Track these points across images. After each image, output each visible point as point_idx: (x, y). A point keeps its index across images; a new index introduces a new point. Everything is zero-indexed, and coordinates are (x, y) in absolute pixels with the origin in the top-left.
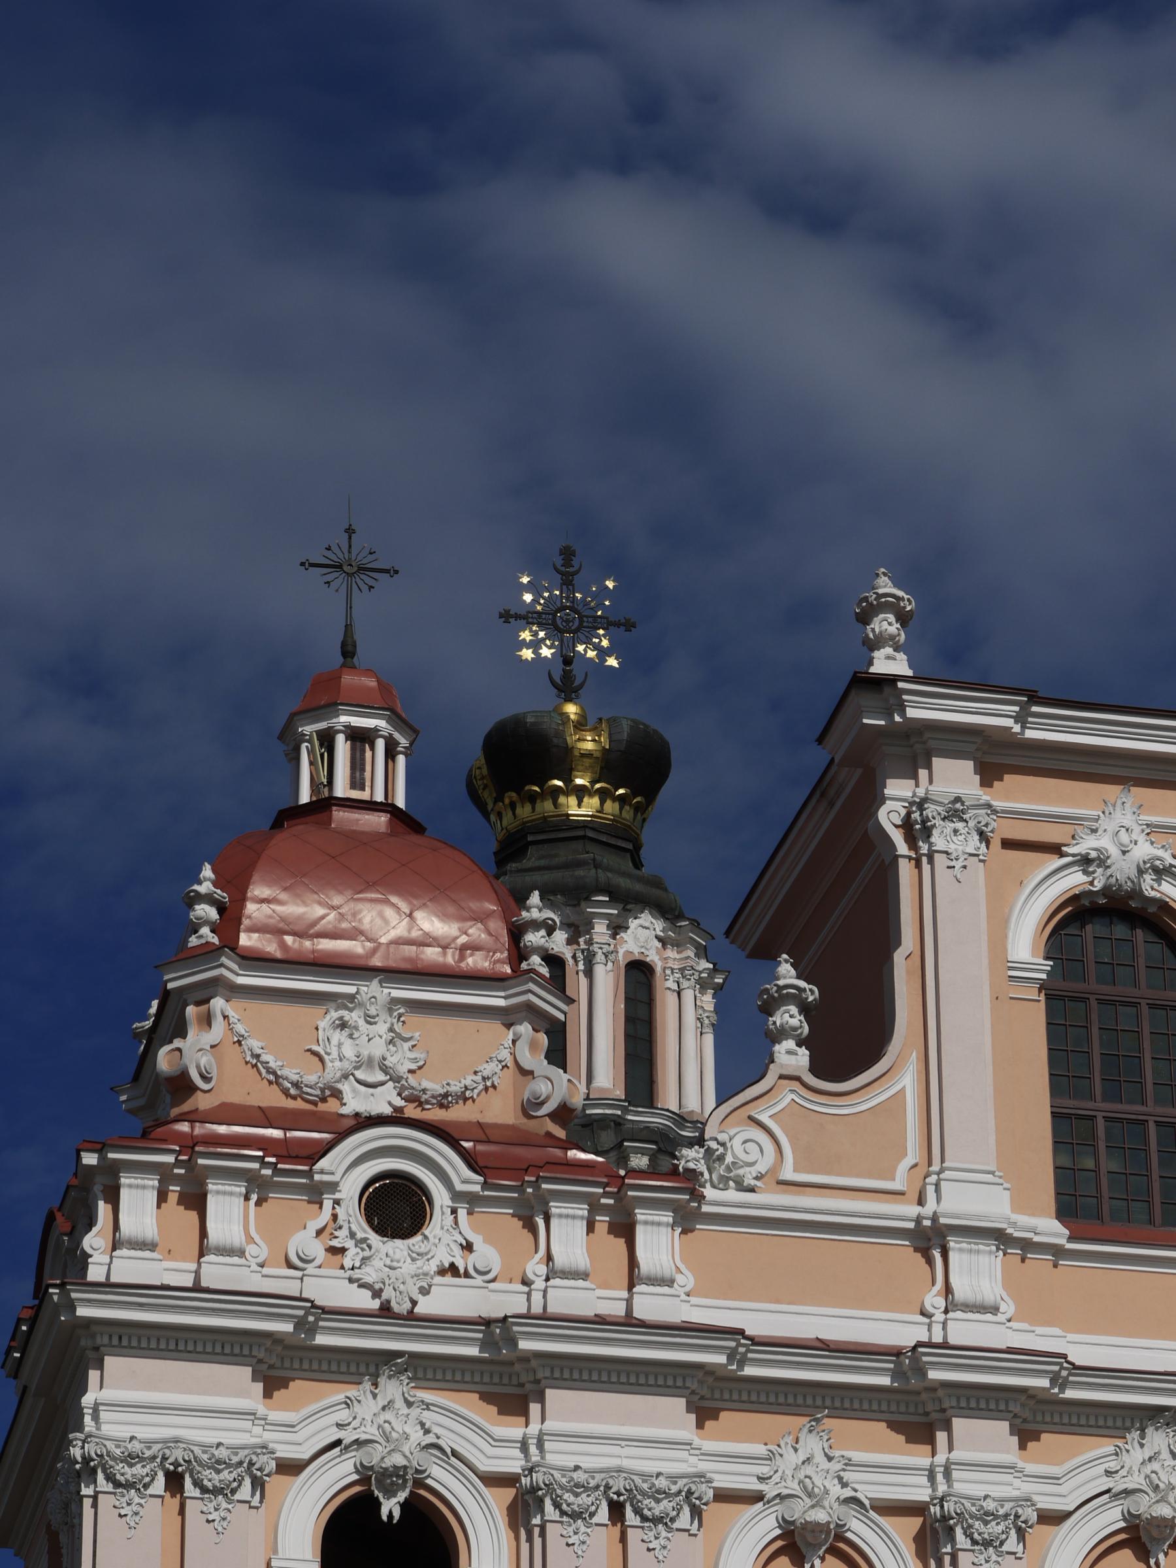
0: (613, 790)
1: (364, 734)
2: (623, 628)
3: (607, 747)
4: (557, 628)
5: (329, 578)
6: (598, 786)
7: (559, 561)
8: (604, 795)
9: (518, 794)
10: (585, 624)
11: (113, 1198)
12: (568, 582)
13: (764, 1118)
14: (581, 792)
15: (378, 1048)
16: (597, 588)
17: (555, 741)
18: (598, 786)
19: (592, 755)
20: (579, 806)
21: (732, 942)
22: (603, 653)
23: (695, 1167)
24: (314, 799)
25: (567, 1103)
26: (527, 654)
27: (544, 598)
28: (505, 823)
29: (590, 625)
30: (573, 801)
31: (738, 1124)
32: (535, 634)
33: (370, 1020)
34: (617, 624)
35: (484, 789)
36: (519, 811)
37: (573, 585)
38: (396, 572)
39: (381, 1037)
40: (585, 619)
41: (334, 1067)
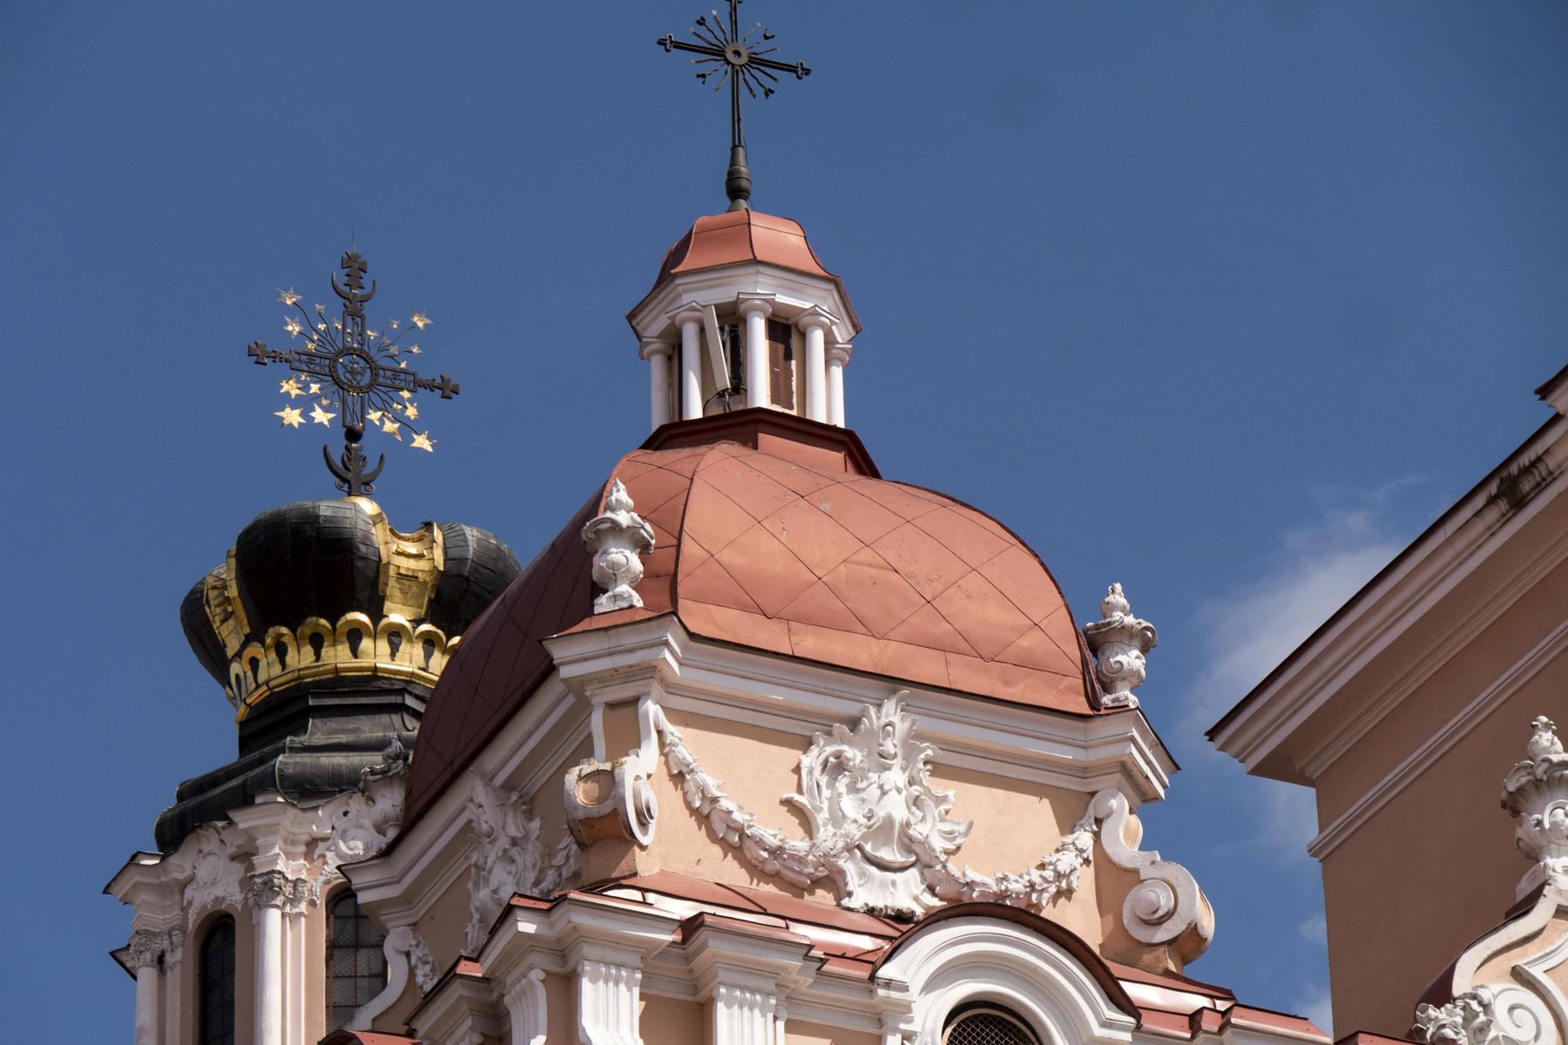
0: (444, 638)
1: (788, 319)
2: (438, 392)
3: (441, 568)
4: (337, 381)
5: (704, 68)
6: (425, 627)
7: (340, 278)
8: (429, 642)
9: (294, 631)
10: (381, 380)
11: (565, 988)
12: (354, 311)
13: (1537, 972)
14: (396, 636)
15: (896, 808)
16: (399, 325)
17: (363, 548)
18: (425, 627)
19: (417, 577)
20: (393, 655)
21: (1222, 748)
22: (409, 427)
23: (1454, 1036)
24: (716, 411)
25: (1199, 927)
26: (292, 417)
27: (317, 332)
28: (262, 677)
29: (389, 382)
30: (383, 646)
31: (1498, 978)
32: (306, 387)
33: (882, 761)
34: (431, 386)
35: (223, 622)
36: (292, 657)
37: (363, 318)
38: (807, 72)
39: (899, 791)
40: (381, 372)
41: (827, 836)
